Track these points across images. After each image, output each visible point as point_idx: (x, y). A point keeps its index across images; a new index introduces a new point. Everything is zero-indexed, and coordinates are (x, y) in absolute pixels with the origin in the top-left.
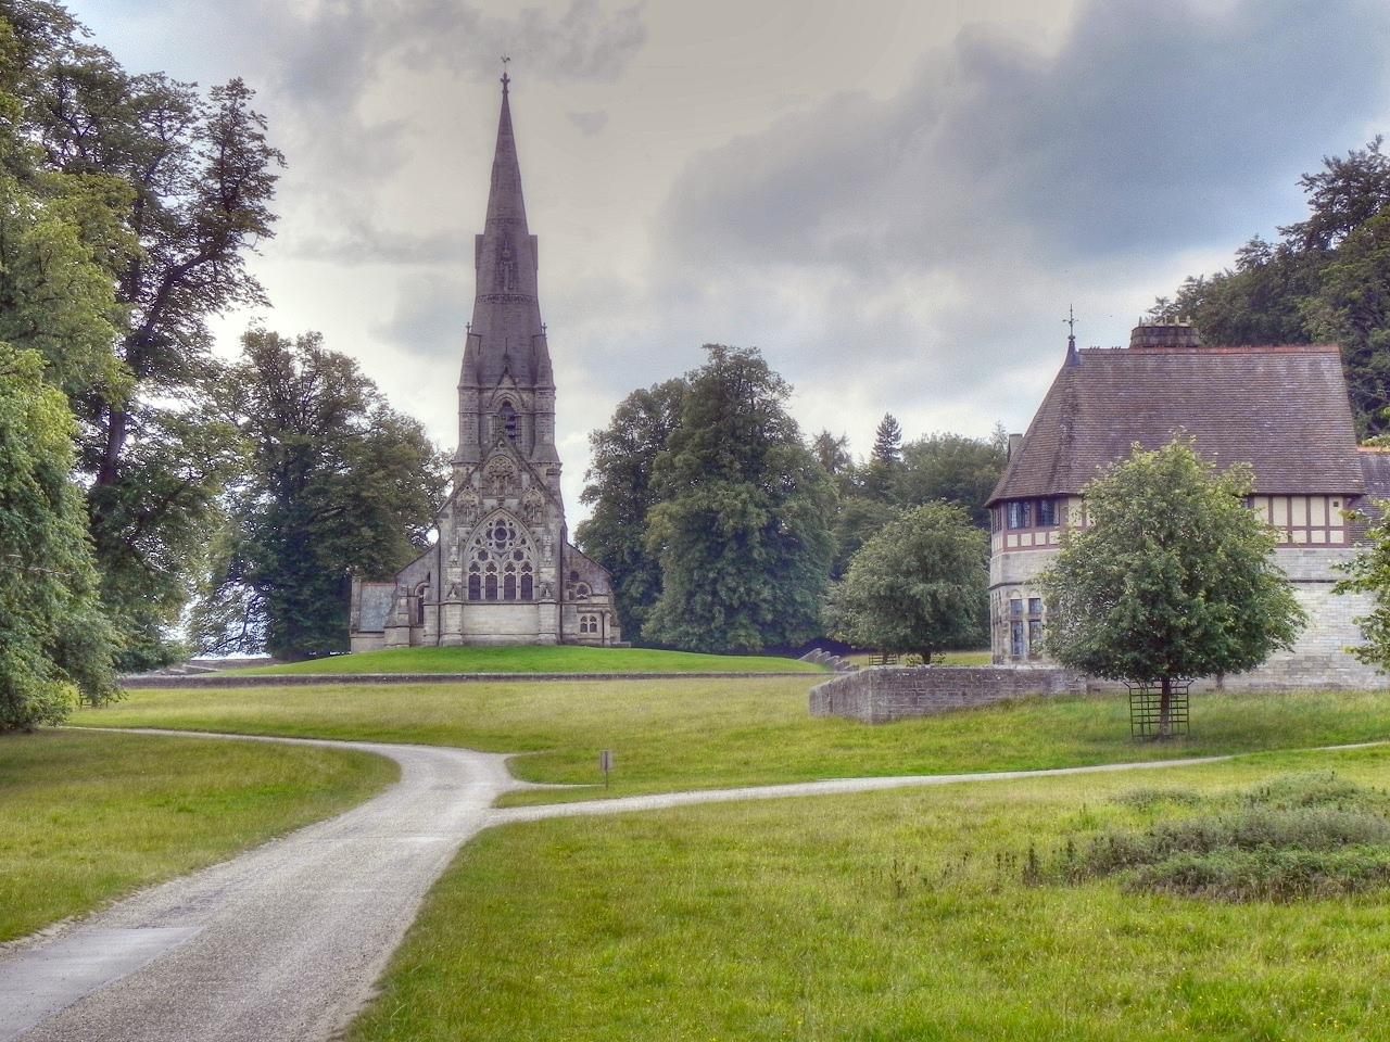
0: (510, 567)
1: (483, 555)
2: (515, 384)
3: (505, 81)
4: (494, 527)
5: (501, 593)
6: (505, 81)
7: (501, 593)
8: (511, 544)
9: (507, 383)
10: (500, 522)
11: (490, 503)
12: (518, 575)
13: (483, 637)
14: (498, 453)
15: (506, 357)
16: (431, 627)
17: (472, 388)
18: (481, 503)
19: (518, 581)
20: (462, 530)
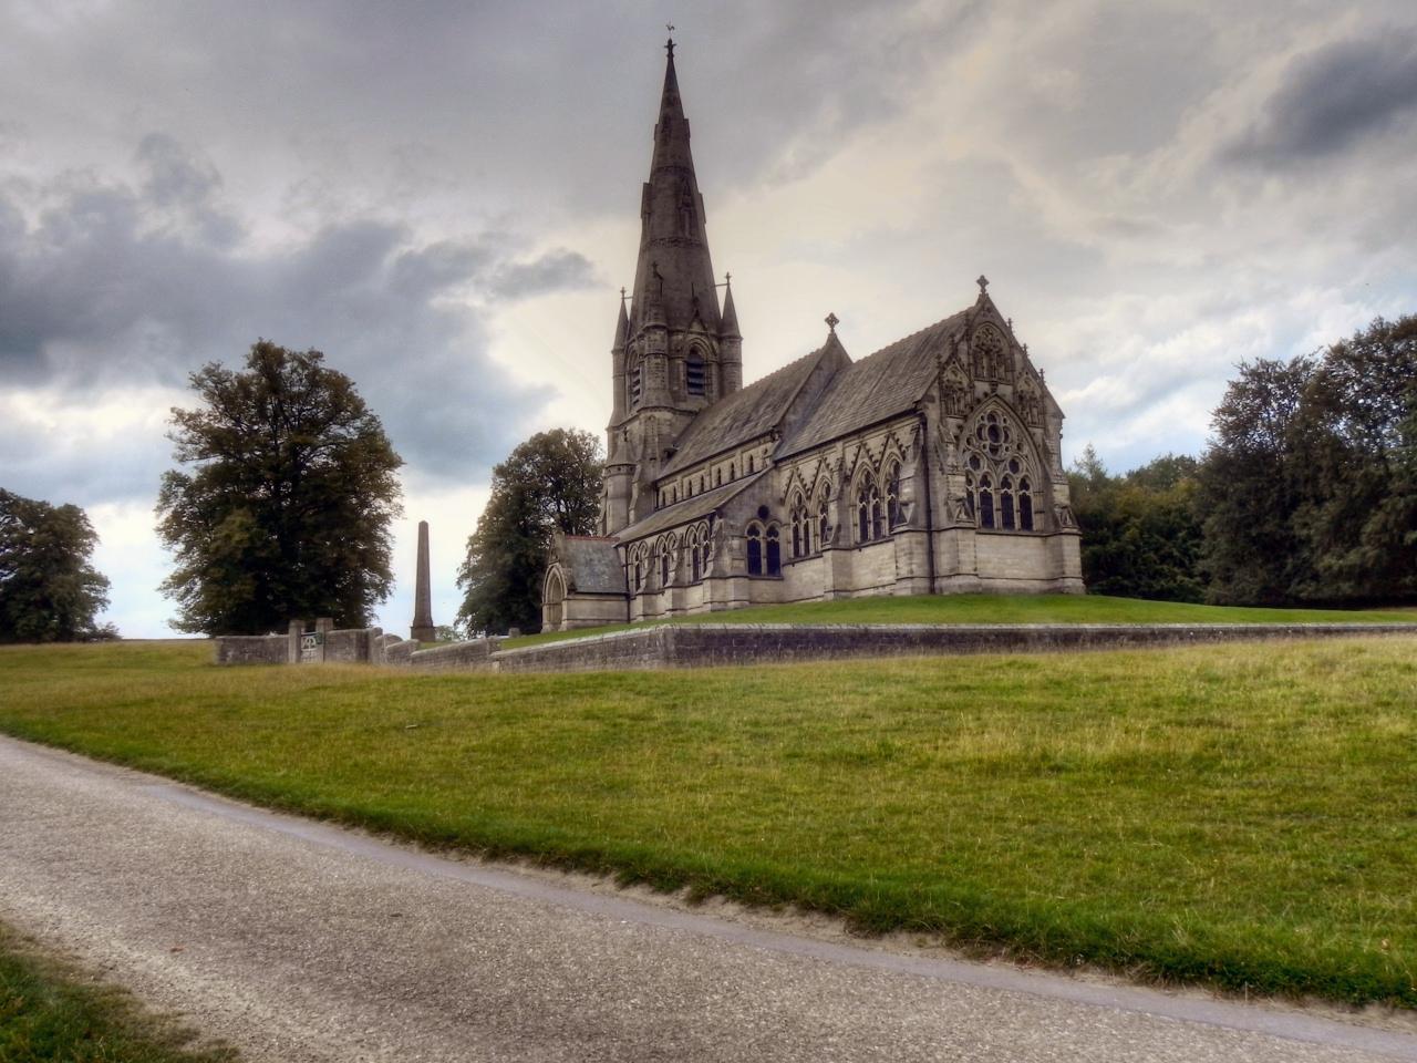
0: (1006, 483)
1: (975, 462)
2: (704, 328)
3: (670, 46)
4: (988, 424)
5: (997, 517)
6: (670, 46)
8: (1007, 449)
9: (696, 327)
10: (992, 417)
11: (982, 387)
12: (1014, 493)
14: (984, 319)
16: (919, 566)
17: (656, 327)
18: (972, 387)
19: (763, 546)
20: (952, 422)
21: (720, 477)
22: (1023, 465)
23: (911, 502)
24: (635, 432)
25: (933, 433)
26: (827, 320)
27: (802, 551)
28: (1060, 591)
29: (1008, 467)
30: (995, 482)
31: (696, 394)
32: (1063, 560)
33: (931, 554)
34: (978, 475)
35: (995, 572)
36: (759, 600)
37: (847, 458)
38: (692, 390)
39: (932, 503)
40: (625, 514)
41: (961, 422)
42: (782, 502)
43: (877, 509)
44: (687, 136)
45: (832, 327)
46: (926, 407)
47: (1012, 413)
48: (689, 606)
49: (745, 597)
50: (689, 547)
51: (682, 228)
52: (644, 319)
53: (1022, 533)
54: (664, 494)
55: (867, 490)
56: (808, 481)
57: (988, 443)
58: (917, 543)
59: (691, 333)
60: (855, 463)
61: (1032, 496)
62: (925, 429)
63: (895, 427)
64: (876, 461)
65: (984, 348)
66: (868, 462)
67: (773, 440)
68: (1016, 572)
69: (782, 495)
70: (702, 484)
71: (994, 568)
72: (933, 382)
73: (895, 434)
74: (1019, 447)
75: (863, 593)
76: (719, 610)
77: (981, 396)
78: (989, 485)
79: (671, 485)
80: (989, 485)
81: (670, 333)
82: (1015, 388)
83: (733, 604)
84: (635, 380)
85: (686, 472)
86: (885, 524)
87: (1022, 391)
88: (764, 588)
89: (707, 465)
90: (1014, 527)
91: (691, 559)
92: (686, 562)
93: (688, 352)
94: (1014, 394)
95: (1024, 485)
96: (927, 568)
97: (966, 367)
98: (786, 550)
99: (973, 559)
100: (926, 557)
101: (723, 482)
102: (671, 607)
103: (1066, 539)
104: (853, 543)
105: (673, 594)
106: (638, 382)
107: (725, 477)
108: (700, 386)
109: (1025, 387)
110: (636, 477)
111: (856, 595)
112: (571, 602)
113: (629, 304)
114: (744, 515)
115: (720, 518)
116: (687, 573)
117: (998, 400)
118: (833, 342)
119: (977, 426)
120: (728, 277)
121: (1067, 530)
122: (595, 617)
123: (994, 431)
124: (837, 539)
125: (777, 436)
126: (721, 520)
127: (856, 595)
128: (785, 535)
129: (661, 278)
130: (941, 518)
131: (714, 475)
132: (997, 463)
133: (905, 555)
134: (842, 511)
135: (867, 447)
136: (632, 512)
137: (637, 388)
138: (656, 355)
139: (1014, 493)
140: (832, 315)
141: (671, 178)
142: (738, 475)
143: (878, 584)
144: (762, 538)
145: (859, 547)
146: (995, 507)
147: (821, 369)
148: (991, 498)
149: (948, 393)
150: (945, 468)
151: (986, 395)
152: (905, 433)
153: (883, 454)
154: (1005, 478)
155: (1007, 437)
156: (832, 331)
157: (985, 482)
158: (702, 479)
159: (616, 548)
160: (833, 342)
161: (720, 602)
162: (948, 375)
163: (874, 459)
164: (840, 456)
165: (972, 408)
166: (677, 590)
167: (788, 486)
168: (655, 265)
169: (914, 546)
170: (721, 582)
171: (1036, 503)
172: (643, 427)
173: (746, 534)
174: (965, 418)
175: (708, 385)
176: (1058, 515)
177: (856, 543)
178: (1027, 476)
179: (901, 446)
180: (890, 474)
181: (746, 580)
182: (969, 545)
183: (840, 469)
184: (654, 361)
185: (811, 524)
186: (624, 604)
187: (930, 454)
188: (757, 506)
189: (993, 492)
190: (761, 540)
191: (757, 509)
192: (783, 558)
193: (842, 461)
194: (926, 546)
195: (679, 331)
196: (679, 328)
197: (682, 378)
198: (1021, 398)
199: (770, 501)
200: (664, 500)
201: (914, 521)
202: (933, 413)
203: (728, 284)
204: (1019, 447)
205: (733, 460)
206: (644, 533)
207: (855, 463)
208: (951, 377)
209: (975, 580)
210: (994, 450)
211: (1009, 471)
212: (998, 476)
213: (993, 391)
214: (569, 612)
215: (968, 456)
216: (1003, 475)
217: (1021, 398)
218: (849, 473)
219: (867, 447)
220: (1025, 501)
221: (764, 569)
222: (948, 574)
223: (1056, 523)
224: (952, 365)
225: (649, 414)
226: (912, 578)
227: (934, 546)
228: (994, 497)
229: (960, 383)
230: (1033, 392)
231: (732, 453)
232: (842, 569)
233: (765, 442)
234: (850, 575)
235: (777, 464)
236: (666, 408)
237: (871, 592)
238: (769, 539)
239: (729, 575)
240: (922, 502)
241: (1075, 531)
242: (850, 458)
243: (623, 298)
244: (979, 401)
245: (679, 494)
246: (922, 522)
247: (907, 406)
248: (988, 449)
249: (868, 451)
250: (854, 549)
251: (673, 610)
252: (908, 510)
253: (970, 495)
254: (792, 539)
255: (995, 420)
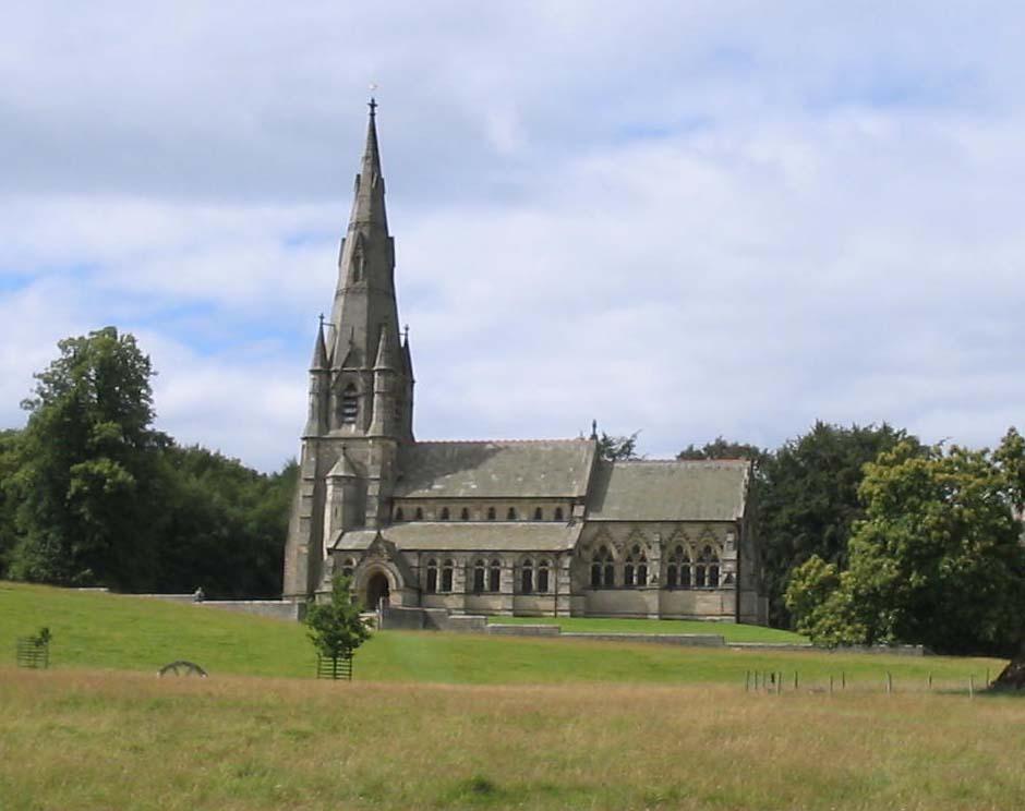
3: (373, 106)
6: (373, 106)
7: (693, 581)
120: (407, 329)
203: (406, 335)
243: (322, 324)
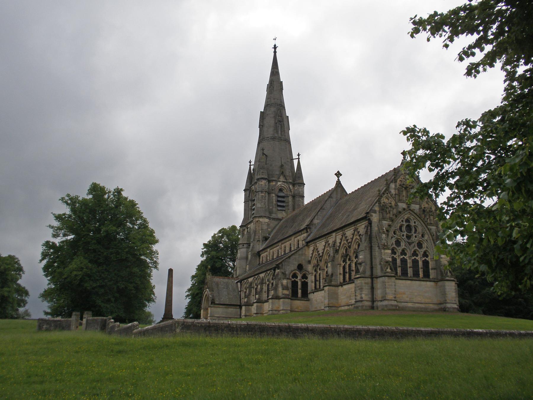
0: (415, 254)
1: (398, 243)
2: (286, 179)
3: (275, 47)
4: (405, 224)
5: (410, 271)
6: (275, 47)
8: (416, 237)
9: (282, 179)
10: (408, 221)
12: (420, 259)
13: (403, 304)
15: (282, 166)
16: (366, 295)
18: (396, 205)
20: (385, 223)
21: (285, 250)
22: (425, 245)
23: (363, 263)
24: (252, 228)
25: (375, 228)
26: (336, 174)
27: (318, 287)
28: (444, 310)
29: (416, 245)
30: (409, 253)
31: (281, 210)
32: (446, 294)
33: (372, 288)
34: (399, 250)
35: (408, 299)
36: (296, 310)
37: (337, 240)
38: (280, 208)
39: (373, 263)
40: (244, 267)
41: (391, 223)
42: (309, 262)
43: (350, 266)
44: (282, 89)
45: (338, 177)
46: (372, 216)
47: (418, 219)
48: (264, 312)
49: (289, 309)
50: (265, 283)
51: (277, 132)
52: (257, 175)
53: (402, 278)
54: (262, 258)
55: (346, 257)
56: (321, 252)
57: (405, 234)
58: (365, 283)
59: (280, 181)
60: (340, 243)
61: (429, 260)
62: (371, 226)
63: (358, 225)
64: (349, 242)
65: (404, 186)
66: (346, 243)
67: (307, 232)
68: (419, 299)
69: (310, 259)
70: (278, 253)
71: (407, 297)
72: (376, 203)
73: (358, 229)
74: (423, 236)
75: (343, 308)
76: (274, 312)
77: (400, 210)
78: (405, 254)
79: (265, 253)
80: (405, 254)
81: (269, 181)
82: (420, 206)
83: (282, 311)
84: (253, 203)
85: (271, 247)
86: (353, 273)
87: (424, 208)
88: (298, 304)
89: (280, 244)
90: (419, 276)
91: (266, 289)
92: (264, 290)
93: (278, 190)
94: (420, 209)
95: (425, 255)
96: (370, 296)
97: (394, 196)
98: (311, 286)
99: (394, 292)
100: (370, 290)
101: (286, 253)
102: (255, 312)
103: (447, 283)
104: (339, 283)
105: (257, 306)
106: (254, 205)
107: (287, 251)
108: (283, 206)
109: (426, 206)
110: (250, 249)
111: (340, 309)
112: (212, 308)
113: (252, 167)
114: (291, 267)
115: (278, 269)
116: (264, 296)
117: (411, 212)
118: (339, 183)
119: (399, 225)
120: (299, 155)
121: (447, 278)
122: (224, 316)
123: (409, 228)
124: (331, 281)
125: (309, 230)
126: (279, 270)
127: (340, 309)
128: (311, 279)
129: (266, 156)
130: (378, 271)
131: (283, 249)
132: (410, 244)
133: (359, 289)
134: (333, 267)
135: (346, 236)
136: (248, 266)
137: (253, 208)
138: (262, 192)
139: (420, 259)
140: (338, 172)
141: (273, 109)
142: (293, 249)
143: (349, 304)
144: (299, 280)
145: (341, 285)
146: (409, 265)
147: (332, 198)
148: (407, 261)
149: (383, 209)
150: (380, 246)
151: (404, 209)
152: (362, 227)
153: (352, 239)
154: (415, 251)
155: (416, 231)
156: (338, 179)
157: (403, 253)
158: (278, 251)
159: (237, 283)
160: (339, 183)
161: (276, 310)
162: (384, 200)
163: (349, 241)
164: (334, 240)
165: (396, 216)
166: (259, 304)
167: (312, 254)
168: (263, 150)
169: (364, 284)
170: (277, 300)
171: (431, 265)
172: (254, 226)
173: (291, 278)
174: (392, 221)
175: (287, 206)
176: (443, 271)
177: (341, 283)
178: (427, 250)
179: (360, 235)
180: (356, 249)
181: (290, 300)
182: (392, 285)
183: (334, 246)
184: (261, 194)
185: (322, 273)
186: (239, 310)
187: (373, 239)
188: (296, 264)
189: (408, 259)
190: (299, 281)
191: (297, 265)
192: (309, 290)
193: (335, 242)
194: (370, 285)
195: (273, 181)
196: (274, 179)
197: (274, 203)
198: (424, 211)
199: (304, 261)
200: (262, 261)
201: (364, 272)
202: (375, 218)
203: (299, 159)
204: (423, 236)
205: (290, 242)
206: (249, 276)
207: (340, 243)
208: (386, 201)
209: (395, 303)
210: (409, 237)
211: (416, 248)
212: (410, 250)
213: (408, 207)
214: (211, 312)
215: (393, 240)
216: (413, 250)
217: (424, 211)
218: (338, 248)
219: (346, 236)
220: (426, 263)
221: (300, 294)
222: (381, 299)
223: (442, 274)
224: (386, 195)
225: (257, 219)
226: (362, 301)
227: (374, 285)
228: (408, 261)
229: (390, 203)
230: (431, 208)
231: (290, 238)
232: (333, 296)
233: (304, 233)
234: (337, 299)
235: (308, 244)
236: (265, 217)
237: (346, 308)
238: (303, 280)
239: (281, 297)
240: (368, 262)
241: (452, 279)
242: (338, 241)
243: (250, 165)
244: (400, 212)
245: (268, 258)
246: (368, 273)
247: (363, 215)
248: (405, 237)
249: (346, 237)
250: (339, 286)
251: (256, 314)
252: (361, 267)
253: (394, 260)
254: (314, 281)
255: (409, 222)
